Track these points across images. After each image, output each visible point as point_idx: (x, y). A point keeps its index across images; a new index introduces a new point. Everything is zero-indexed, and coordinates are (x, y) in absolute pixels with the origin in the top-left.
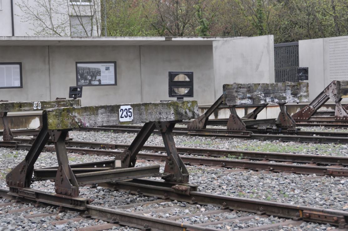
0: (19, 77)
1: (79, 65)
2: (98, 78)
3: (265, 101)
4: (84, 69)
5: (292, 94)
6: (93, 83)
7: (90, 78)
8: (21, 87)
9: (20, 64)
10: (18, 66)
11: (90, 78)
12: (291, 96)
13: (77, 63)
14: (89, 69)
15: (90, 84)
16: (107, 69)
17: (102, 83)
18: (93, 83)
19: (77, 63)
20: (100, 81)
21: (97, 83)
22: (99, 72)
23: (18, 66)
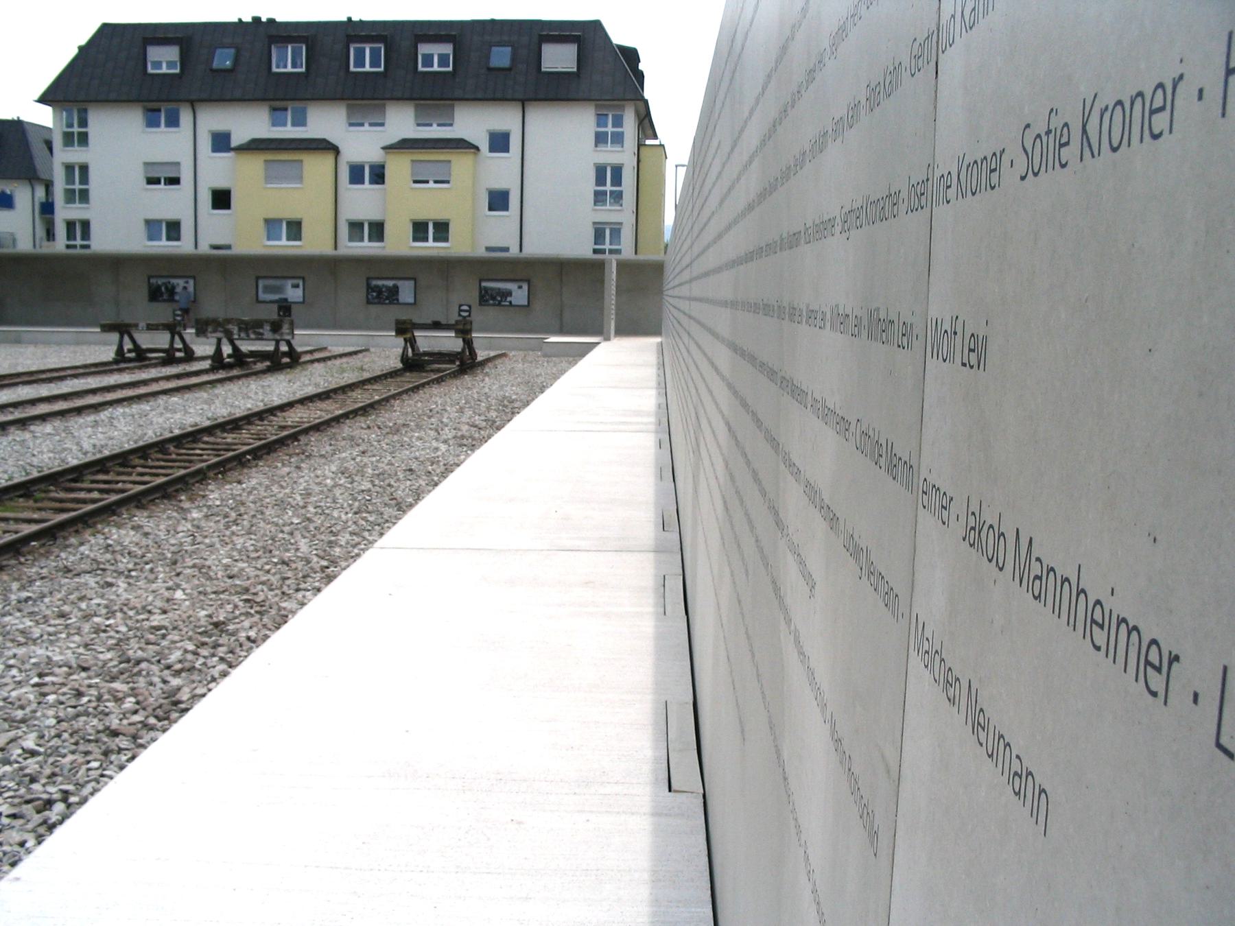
0: (413, 295)
1: (484, 284)
2: (509, 299)
3: (239, 336)
4: (492, 289)
5: (271, 330)
6: (503, 303)
7: (499, 299)
8: (415, 303)
9: (415, 279)
10: (412, 282)
11: (499, 299)
12: (271, 333)
13: (481, 281)
14: (499, 289)
15: (499, 304)
16: (520, 287)
17: (513, 303)
18: (503, 303)
19: (481, 281)
20: (510, 302)
21: (508, 303)
22: (509, 293)
23: (412, 282)
